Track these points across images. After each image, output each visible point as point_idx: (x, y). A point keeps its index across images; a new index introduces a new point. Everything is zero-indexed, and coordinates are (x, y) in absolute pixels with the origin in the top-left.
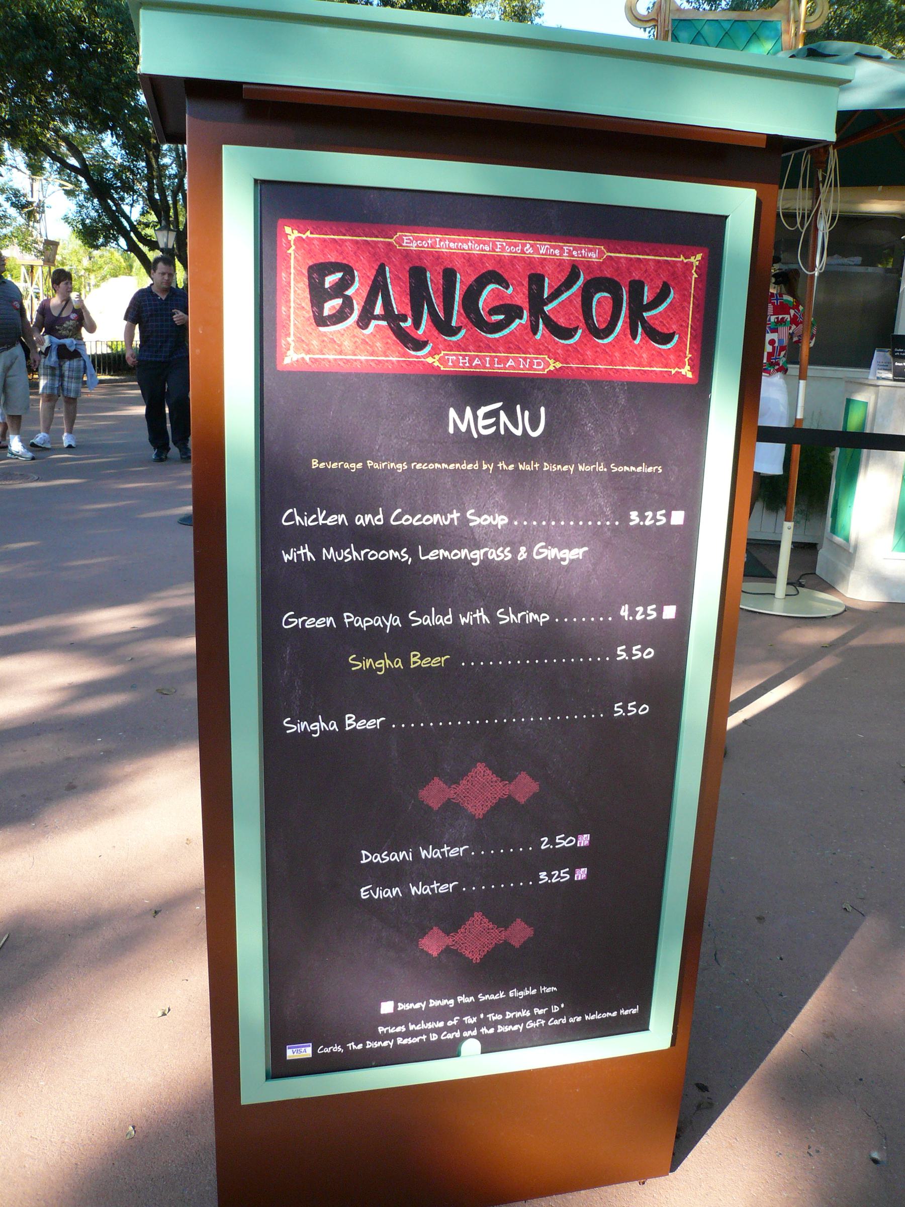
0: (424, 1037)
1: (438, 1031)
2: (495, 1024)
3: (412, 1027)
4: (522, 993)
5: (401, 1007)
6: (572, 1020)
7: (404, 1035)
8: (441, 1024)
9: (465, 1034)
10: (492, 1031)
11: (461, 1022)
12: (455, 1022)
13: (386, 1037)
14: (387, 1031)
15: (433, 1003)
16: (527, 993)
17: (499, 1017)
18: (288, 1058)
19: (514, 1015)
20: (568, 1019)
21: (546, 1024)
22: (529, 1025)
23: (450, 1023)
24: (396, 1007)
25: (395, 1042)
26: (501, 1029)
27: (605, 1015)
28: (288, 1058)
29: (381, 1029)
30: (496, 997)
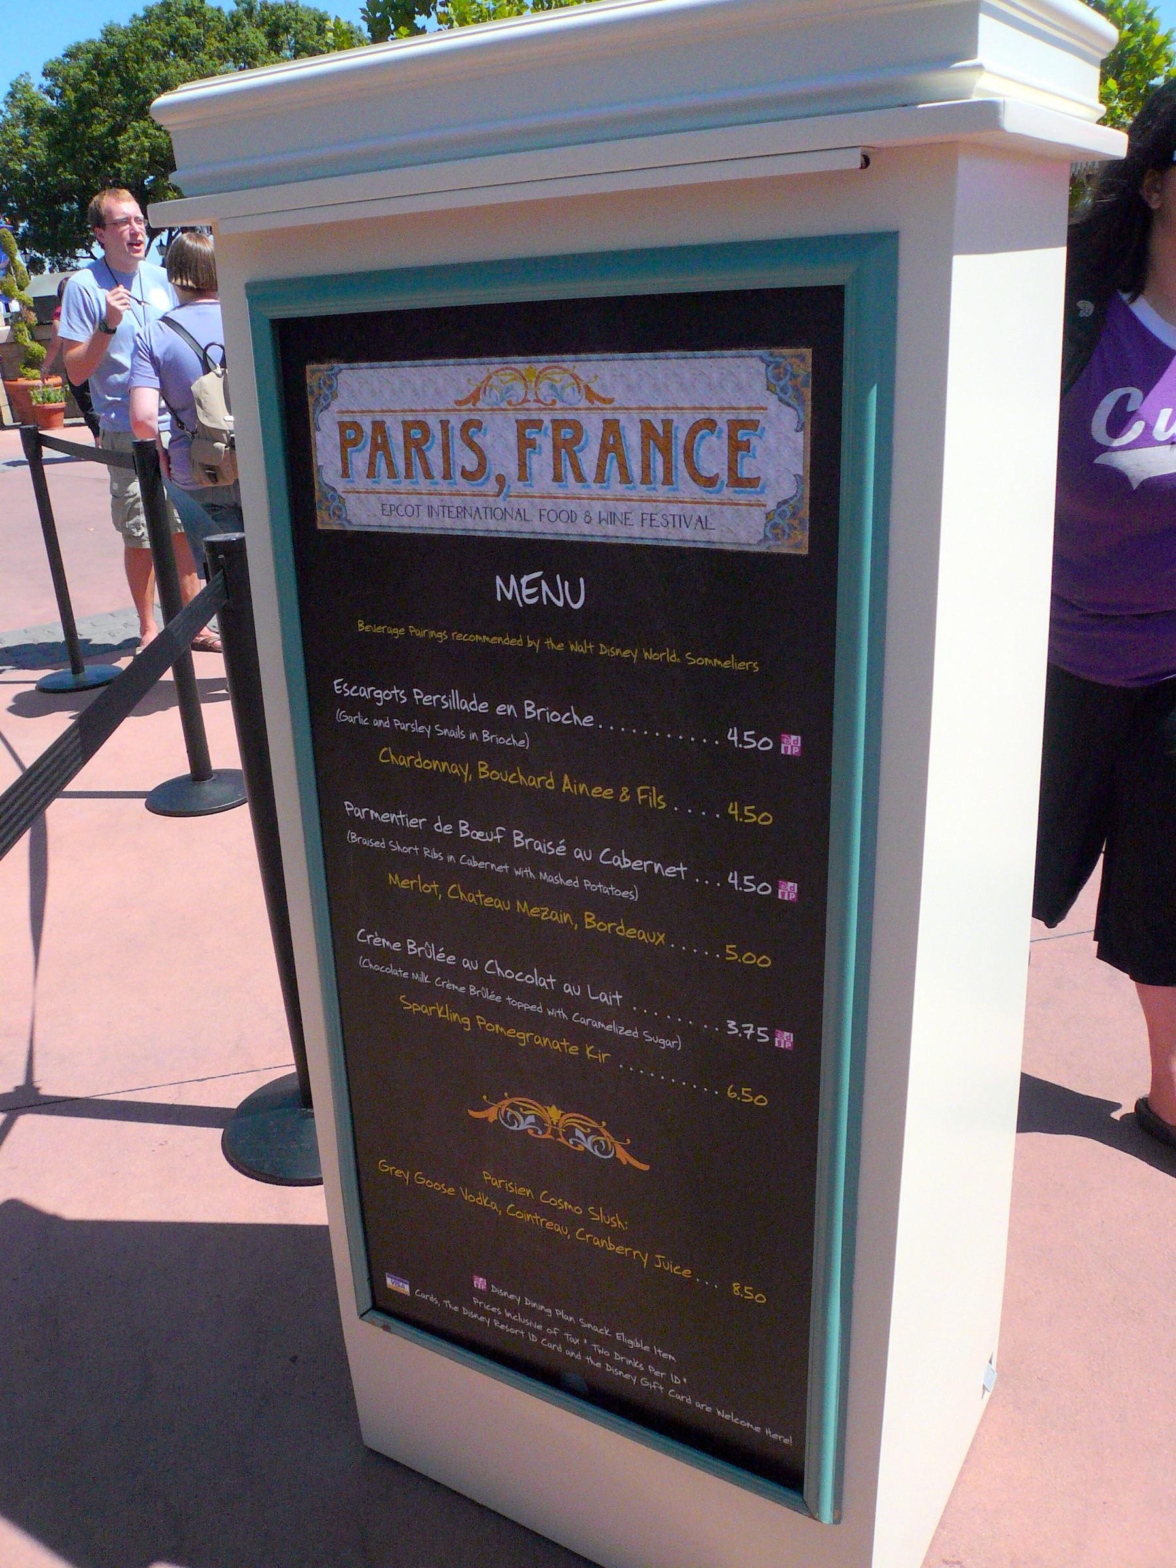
2: (603, 1359)
4: (631, 1342)
5: (494, 1289)
7: (503, 1320)
10: (598, 1365)
11: (561, 1334)
13: (480, 1311)
14: (482, 1305)
16: (638, 1345)
26: (609, 1368)
30: (600, 1331)
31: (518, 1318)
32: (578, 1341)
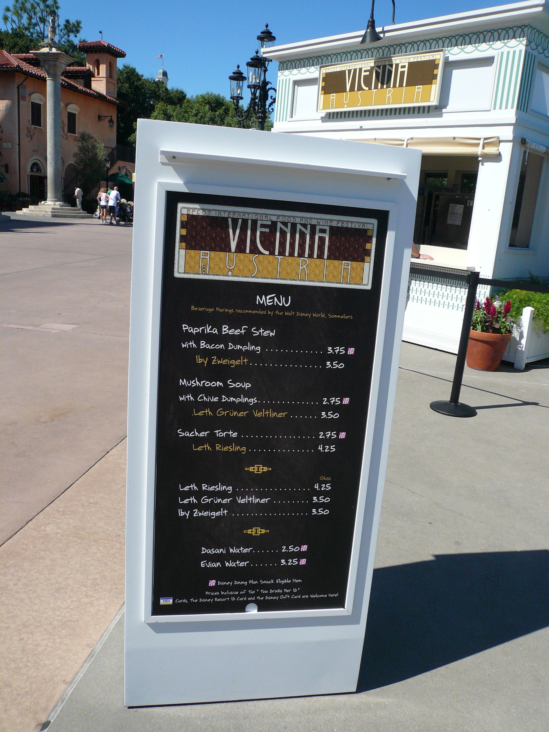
0: (228, 599)
1: (236, 596)
2: (264, 595)
3: (222, 593)
6: (303, 597)
7: (218, 597)
8: (237, 593)
9: (249, 599)
10: (262, 598)
12: (244, 592)
14: (210, 594)
15: (236, 583)
17: (266, 592)
18: (161, 604)
19: (274, 591)
20: (301, 596)
21: (290, 597)
22: (281, 597)
23: (241, 593)
24: (217, 583)
25: (214, 600)
26: (267, 598)
27: (320, 596)
28: (161, 604)
29: (207, 593)
31: (227, 593)
32: (254, 592)
